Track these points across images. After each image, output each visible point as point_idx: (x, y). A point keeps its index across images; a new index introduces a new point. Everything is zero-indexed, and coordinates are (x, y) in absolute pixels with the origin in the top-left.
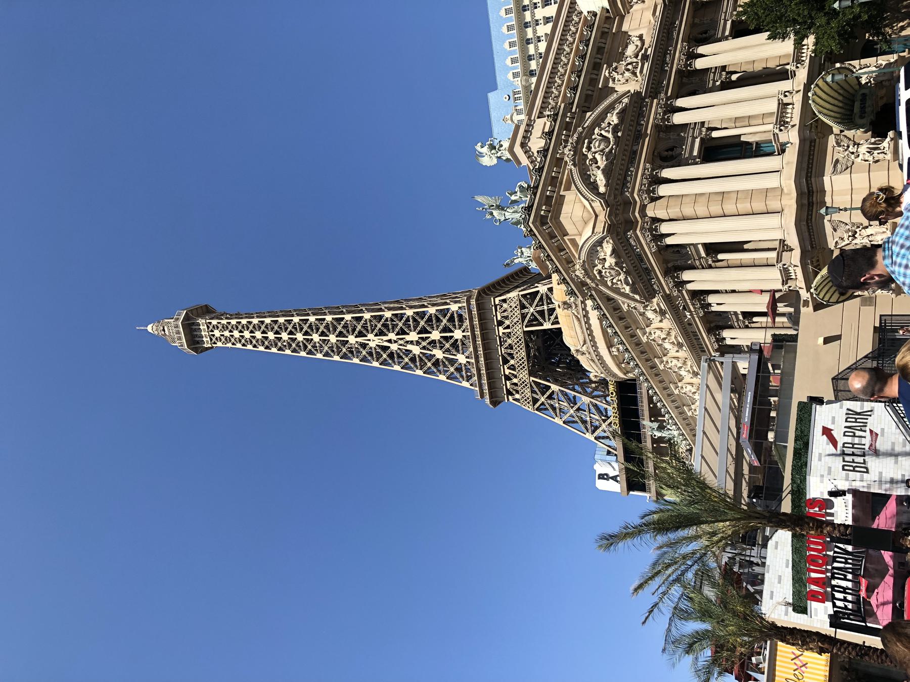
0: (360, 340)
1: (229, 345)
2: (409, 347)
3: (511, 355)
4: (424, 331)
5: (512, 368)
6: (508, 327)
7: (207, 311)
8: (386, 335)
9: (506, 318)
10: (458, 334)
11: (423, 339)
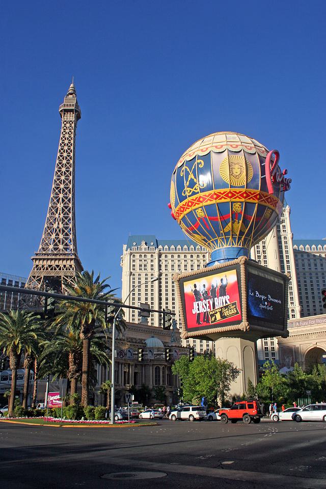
0: (61, 199)
1: (62, 130)
2: (57, 223)
3: (52, 269)
4: (63, 231)
6: (63, 270)
7: (78, 117)
9: (67, 269)
10: (61, 247)
11: (60, 231)
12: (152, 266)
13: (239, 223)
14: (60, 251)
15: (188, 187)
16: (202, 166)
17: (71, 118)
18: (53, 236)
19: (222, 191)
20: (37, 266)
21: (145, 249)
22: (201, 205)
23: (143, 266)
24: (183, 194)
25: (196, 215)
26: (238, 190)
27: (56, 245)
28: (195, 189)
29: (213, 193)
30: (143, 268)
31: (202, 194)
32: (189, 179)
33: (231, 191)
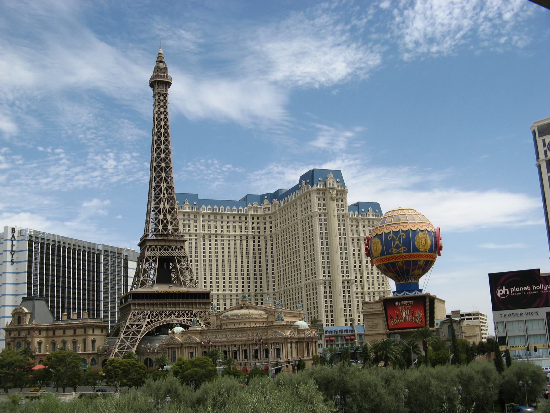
2: (162, 203)
3: (165, 250)
10: (170, 227)
12: (196, 226)
17: (165, 90)
18: (161, 217)
19: (416, 253)
20: (150, 246)
21: (189, 208)
22: (402, 260)
23: (187, 226)
27: (165, 225)
30: (187, 228)
31: (404, 254)
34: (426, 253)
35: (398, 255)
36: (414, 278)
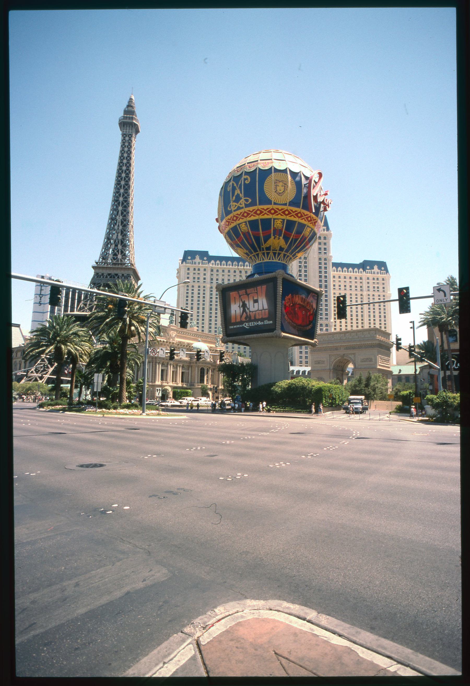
0: (120, 212)
3: (111, 277)
5: (106, 277)
8: (121, 224)
10: (120, 256)
11: (119, 242)
13: (279, 239)
14: (118, 260)
15: (234, 201)
16: (248, 182)
17: (130, 131)
19: (265, 207)
22: (245, 220)
23: (196, 278)
24: (229, 209)
25: (240, 229)
26: (280, 207)
28: (240, 204)
29: (257, 209)
30: (196, 280)
32: (236, 194)
33: (274, 208)
34: (285, 207)
35: (238, 212)
36: (275, 254)
